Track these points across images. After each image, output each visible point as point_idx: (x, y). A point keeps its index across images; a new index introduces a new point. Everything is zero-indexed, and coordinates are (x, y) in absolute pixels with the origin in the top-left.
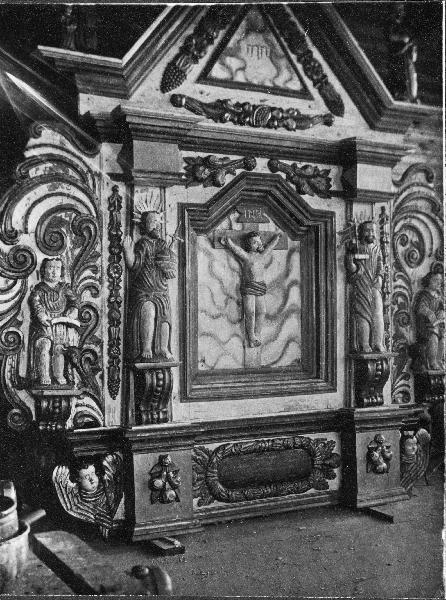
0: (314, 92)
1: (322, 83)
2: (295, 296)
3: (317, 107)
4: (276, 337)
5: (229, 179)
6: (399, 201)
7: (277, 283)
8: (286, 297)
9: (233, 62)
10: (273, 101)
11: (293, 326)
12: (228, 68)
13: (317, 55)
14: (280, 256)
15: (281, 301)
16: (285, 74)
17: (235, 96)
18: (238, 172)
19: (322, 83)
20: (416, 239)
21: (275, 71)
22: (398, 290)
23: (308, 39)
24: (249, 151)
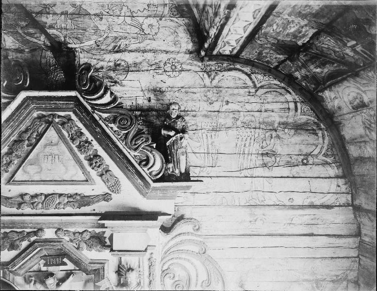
0: (98, 180)
1: (105, 173)
5: (25, 244)
19: (105, 173)
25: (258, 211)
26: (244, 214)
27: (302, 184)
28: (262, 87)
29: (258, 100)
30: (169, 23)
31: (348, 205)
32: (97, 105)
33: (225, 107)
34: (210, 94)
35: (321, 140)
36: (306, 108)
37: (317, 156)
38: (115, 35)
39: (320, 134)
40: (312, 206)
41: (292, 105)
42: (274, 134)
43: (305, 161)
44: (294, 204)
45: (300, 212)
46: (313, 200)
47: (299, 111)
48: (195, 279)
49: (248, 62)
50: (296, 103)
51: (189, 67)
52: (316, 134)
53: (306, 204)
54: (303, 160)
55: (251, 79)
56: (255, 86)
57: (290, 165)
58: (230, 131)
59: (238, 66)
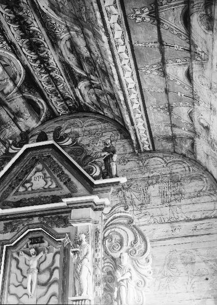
0: (64, 187)
1: (68, 182)
2: (56, 274)
3: (66, 190)
4: (46, 292)
6: (107, 223)
7: (48, 268)
8: (51, 275)
9: (28, 185)
10: (48, 194)
11: (55, 288)
12: (26, 187)
13: (66, 172)
14: (50, 256)
15: (49, 276)
16: (49, 183)
17: (28, 196)
18: (25, 224)
19: (68, 182)
21: (45, 183)
22: (106, 264)
23: (63, 167)
24: (30, 216)
25: (176, 225)
26: (167, 227)
27: (198, 207)
29: (169, 169)
30: (121, 143)
33: (151, 175)
34: (143, 170)
36: (195, 168)
38: (96, 151)
39: (205, 180)
40: (206, 218)
41: (187, 169)
42: (179, 183)
43: (199, 195)
44: (196, 218)
45: (201, 222)
47: (191, 171)
49: (159, 151)
51: (131, 159)
52: (202, 180)
53: (202, 217)
55: (163, 160)
56: (165, 162)
57: (190, 198)
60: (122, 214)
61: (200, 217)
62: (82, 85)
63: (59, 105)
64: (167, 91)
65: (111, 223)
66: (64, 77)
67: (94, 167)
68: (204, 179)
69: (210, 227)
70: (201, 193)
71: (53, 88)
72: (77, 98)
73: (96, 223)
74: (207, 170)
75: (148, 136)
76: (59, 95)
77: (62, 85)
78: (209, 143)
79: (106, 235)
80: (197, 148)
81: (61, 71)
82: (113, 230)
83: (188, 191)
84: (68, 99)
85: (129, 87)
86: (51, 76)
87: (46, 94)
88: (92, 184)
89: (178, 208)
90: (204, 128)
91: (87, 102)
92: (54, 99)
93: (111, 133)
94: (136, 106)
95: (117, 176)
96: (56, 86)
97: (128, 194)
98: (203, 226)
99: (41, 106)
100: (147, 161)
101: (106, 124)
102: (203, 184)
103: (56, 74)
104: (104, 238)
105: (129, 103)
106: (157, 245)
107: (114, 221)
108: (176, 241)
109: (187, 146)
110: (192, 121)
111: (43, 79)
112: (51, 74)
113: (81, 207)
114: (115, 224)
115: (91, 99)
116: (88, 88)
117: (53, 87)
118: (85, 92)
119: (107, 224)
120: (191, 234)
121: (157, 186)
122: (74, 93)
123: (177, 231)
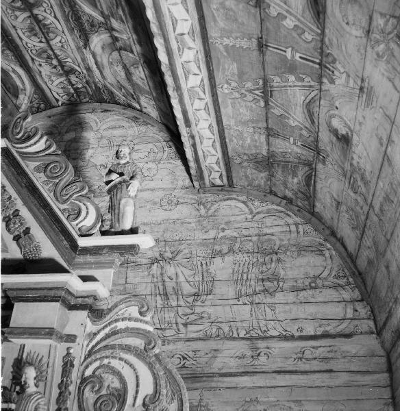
6: (94, 342)
13: (25, 213)
20: (116, 384)
25: (261, 344)
27: (311, 310)
28: (258, 213)
29: (256, 225)
31: (372, 333)
32: (26, 153)
34: (205, 223)
35: (329, 261)
36: (309, 228)
37: (325, 279)
40: (326, 336)
41: (293, 228)
42: (275, 257)
43: (313, 285)
44: (304, 333)
46: (328, 328)
48: (134, 392)
50: (297, 225)
53: (319, 333)
54: (310, 283)
55: (248, 206)
56: (251, 213)
58: (226, 258)
59: (234, 196)
60: (132, 324)
61: (313, 333)
62: (98, 40)
63: (56, 83)
64: (262, 46)
65: (103, 344)
66: (62, 21)
67: (81, 204)
68: (327, 254)
69: (330, 355)
70: (318, 281)
71: (42, 45)
72: (89, 69)
73: (71, 338)
74: (333, 234)
75: (220, 155)
76: (55, 62)
77: (58, 39)
78: (345, 175)
79: (88, 372)
80: (319, 186)
81: (56, 8)
82: (106, 361)
83: (291, 274)
84: (72, 71)
85: (179, 31)
86: (35, 17)
87: (28, 58)
88: (74, 245)
89: (267, 309)
90: (338, 138)
91: (109, 80)
92: (46, 70)
93: (151, 146)
94: (194, 81)
95: (133, 231)
96: (48, 42)
97: (170, 270)
98: (318, 352)
99: (19, 83)
100: (216, 206)
101: (143, 129)
102: (324, 264)
103: (45, 14)
104: (84, 381)
105: (180, 71)
106: (220, 385)
107: (109, 341)
108: (258, 381)
109: (295, 181)
110: (313, 122)
111: (18, 23)
112: (35, 12)
113: (34, 300)
114: (113, 347)
115: (115, 74)
116: (108, 50)
117: (41, 42)
118: (104, 59)
119: (94, 347)
120: (290, 368)
121: (229, 259)
122: (84, 60)
123: (263, 359)
